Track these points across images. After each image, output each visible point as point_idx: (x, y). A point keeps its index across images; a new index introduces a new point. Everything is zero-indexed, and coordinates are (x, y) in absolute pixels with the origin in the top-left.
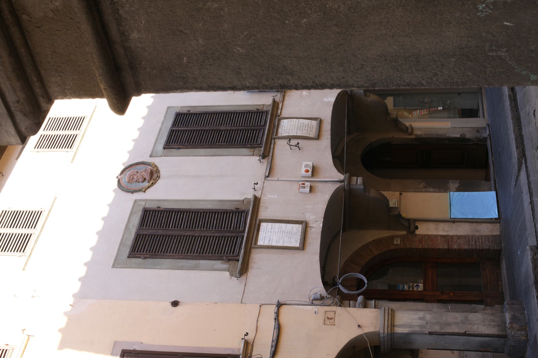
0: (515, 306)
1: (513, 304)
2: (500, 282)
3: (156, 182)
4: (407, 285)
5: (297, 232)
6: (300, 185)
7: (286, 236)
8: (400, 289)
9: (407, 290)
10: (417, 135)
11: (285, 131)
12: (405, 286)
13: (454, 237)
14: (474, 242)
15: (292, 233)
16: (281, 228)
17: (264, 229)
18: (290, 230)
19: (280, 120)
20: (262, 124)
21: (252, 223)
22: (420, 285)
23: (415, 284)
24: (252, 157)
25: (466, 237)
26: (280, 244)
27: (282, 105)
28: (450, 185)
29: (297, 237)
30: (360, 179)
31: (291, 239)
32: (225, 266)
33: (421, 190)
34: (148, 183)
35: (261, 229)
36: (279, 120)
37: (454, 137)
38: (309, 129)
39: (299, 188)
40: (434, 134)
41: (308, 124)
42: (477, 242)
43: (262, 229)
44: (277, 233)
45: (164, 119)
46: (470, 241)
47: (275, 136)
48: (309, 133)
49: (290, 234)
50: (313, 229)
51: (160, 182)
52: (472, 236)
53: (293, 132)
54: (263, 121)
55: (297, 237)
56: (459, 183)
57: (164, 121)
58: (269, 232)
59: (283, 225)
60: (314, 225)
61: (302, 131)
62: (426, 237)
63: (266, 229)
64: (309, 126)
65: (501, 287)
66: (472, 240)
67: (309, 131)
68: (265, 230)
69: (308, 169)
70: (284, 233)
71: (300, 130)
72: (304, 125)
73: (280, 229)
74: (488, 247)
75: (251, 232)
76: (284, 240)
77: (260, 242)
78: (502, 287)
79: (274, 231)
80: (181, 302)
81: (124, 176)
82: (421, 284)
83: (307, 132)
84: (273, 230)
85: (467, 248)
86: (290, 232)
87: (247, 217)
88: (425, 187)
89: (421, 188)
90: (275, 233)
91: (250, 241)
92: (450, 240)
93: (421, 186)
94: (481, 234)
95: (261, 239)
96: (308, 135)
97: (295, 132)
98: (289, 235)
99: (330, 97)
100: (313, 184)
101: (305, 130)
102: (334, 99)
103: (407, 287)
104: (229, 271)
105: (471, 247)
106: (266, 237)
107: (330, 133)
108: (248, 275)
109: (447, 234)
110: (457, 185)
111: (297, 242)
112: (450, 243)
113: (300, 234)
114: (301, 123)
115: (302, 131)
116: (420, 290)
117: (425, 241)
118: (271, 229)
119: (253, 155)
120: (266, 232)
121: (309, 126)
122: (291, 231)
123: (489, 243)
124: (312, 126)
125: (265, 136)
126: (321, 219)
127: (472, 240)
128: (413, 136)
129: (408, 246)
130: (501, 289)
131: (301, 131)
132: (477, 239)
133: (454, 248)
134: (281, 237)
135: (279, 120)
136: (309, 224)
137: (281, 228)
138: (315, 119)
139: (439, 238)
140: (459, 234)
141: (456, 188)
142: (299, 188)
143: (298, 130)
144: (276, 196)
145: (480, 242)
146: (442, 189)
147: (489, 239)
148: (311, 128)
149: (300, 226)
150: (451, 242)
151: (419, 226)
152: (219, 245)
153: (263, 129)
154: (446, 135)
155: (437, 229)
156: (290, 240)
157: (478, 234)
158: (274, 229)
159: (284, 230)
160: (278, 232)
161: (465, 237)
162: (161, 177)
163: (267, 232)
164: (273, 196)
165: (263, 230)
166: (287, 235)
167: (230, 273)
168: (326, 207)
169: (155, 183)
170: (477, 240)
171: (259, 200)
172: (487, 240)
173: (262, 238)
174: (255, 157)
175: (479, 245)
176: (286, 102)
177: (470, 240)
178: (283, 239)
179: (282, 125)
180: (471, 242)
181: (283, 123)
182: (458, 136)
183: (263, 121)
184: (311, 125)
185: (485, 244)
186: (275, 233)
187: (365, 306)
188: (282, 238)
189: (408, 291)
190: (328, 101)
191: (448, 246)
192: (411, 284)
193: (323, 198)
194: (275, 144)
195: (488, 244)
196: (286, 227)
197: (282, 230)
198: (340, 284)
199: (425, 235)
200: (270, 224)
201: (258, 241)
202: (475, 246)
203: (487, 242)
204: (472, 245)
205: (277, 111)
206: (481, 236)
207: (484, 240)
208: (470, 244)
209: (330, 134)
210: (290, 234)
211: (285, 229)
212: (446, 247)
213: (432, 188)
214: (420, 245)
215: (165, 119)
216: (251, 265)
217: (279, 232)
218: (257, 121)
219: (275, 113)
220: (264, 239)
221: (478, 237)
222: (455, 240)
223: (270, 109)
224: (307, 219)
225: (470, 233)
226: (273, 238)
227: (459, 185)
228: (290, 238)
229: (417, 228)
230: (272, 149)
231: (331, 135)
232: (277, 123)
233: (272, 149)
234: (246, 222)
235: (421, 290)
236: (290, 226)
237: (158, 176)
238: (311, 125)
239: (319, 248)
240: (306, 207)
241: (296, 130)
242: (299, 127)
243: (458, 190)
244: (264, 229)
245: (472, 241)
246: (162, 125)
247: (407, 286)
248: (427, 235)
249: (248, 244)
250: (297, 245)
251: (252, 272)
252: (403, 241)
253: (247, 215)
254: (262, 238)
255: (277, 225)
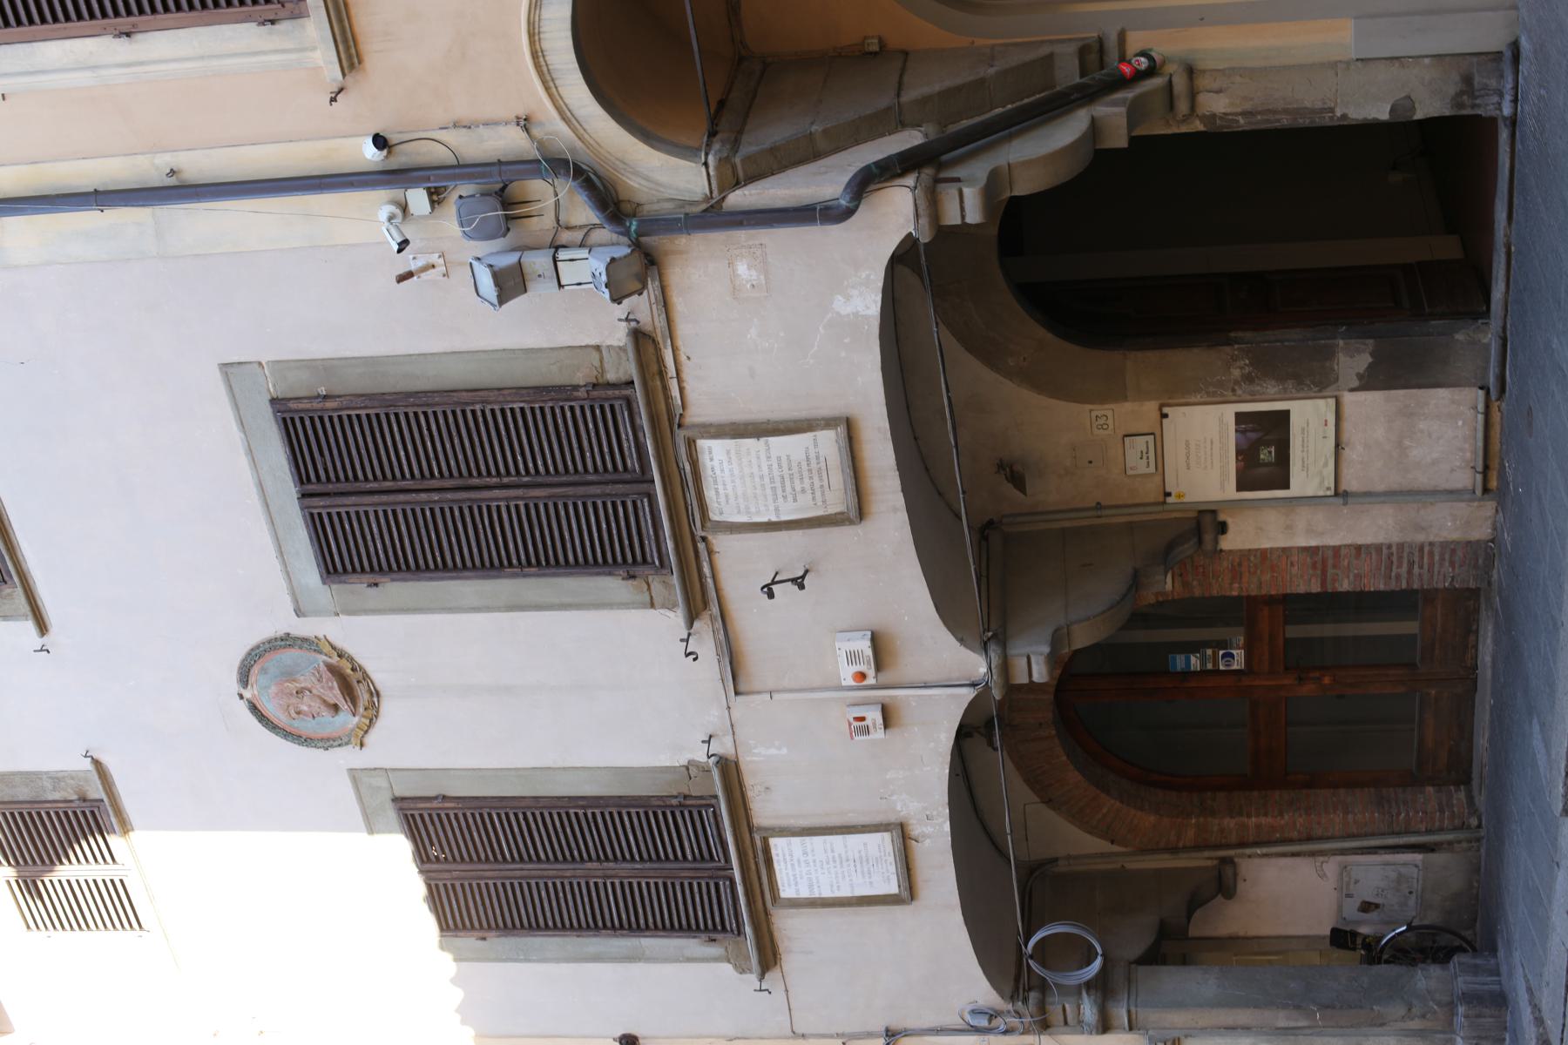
0: (1483, 1020)
1: (1478, 1016)
2: (1472, 638)
3: (378, 712)
4: (1198, 655)
5: (883, 854)
6: (850, 725)
7: (853, 869)
8: (1179, 669)
9: (1199, 669)
10: (1214, 116)
11: (732, 500)
12: (1193, 659)
13: (1343, 552)
14: (1405, 565)
15: (867, 860)
16: (833, 851)
17: (784, 855)
18: (860, 852)
19: (694, 441)
20: (633, 462)
21: (743, 842)
22: (1234, 652)
23: (1221, 652)
24: (652, 611)
25: (1381, 549)
26: (845, 892)
27: (675, 350)
28: (1338, 364)
29: (888, 871)
30: (1038, 664)
31: (870, 877)
32: (714, 950)
33: (1234, 390)
34: (354, 715)
35: (775, 858)
36: (690, 446)
37: (1365, 119)
38: (817, 484)
39: (851, 734)
40: (1286, 111)
41: (808, 459)
42: (1416, 566)
43: (777, 855)
44: (825, 866)
45: (243, 436)
46: (1392, 562)
47: (703, 526)
48: (824, 502)
49: (865, 864)
50: (928, 842)
51: (387, 707)
52: (1401, 546)
53: (762, 508)
54: (630, 448)
55: (888, 871)
56: (1372, 354)
57: (249, 445)
58: (803, 864)
59: (837, 840)
60: (924, 829)
61: (795, 500)
62: (1252, 558)
63: (791, 855)
64: (814, 465)
65: (1473, 651)
66: (1400, 558)
67: (818, 494)
68: (788, 858)
69: (862, 668)
70: (845, 864)
71: (785, 497)
72: (795, 469)
73: (830, 855)
74: (1447, 584)
75: (749, 869)
76: (851, 880)
77: (786, 892)
78: (1477, 650)
79: (814, 861)
80: (644, 1038)
81: (259, 692)
82: (1239, 651)
83: (814, 499)
84: (810, 858)
85: (1382, 587)
86: (861, 857)
87: (721, 826)
88: (1249, 379)
89: (1236, 382)
90: (818, 864)
91: (758, 892)
92: (1330, 562)
93: (1236, 373)
94: (1432, 538)
95: (786, 882)
96: (820, 512)
97: (772, 508)
98: (862, 866)
99: (855, 292)
100: (886, 701)
101: (803, 491)
102: (875, 302)
103: (1198, 662)
104: (729, 961)
105: (1393, 586)
106: (798, 879)
107: (897, 482)
108: (784, 969)
109: (1321, 544)
110: (1363, 361)
111: (889, 882)
112: (1330, 571)
113: (891, 859)
114: (779, 459)
115: (795, 500)
116: (1235, 667)
117: (1252, 570)
118: (805, 853)
119: (652, 605)
120: (793, 865)
121: (814, 465)
122: (863, 854)
123: (1454, 569)
124: (823, 465)
125: (670, 545)
126: (940, 809)
127: (1400, 558)
128: (1198, 126)
129: (1197, 592)
130: (1472, 659)
131: (790, 498)
132: (1417, 554)
133: (1340, 589)
134: (840, 875)
135: (691, 443)
136: (910, 828)
137: (833, 851)
138: (829, 423)
139: (1295, 559)
140: (1360, 541)
141: (1360, 376)
142: (851, 734)
143: (781, 500)
144: (784, 751)
145: (1426, 566)
146: (1308, 382)
147: (1453, 551)
148: (824, 474)
149: (887, 836)
150: (1335, 566)
151: (1229, 521)
152: (673, 904)
153: (645, 500)
154: (1332, 110)
155: (1289, 527)
156: (868, 880)
157: (1421, 538)
158: (814, 855)
159: (844, 856)
160: (828, 863)
161: (1378, 548)
162: (382, 693)
163: (796, 864)
164: (773, 751)
165: (781, 858)
166: (855, 866)
167: (735, 967)
168: (947, 771)
169: (376, 717)
170: (1416, 559)
171: (733, 764)
172: (1447, 556)
173: (789, 880)
174: (662, 611)
175: (1420, 575)
176: (683, 329)
177: (1395, 559)
178: (847, 879)
179: (709, 472)
180: (1394, 567)
181: (711, 460)
182: (1383, 115)
183: (630, 448)
184: (818, 458)
185: (1439, 572)
186: (818, 864)
187: (1105, 1026)
188: (844, 877)
189: (1204, 673)
190: (856, 314)
191: (1324, 583)
192: (1209, 652)
193: (932, 745)
194: (710, 552)
195: (1450, 570)
196: (846, 847)
197: (836, 855)
198: (1031, 957)
199: (1250, 550)
200: (796, 841)
201: (778, 890)
202: (1408, 583)
203: (1447, 564)
204: (1398, 577)
205: (665, 388)
206: (1431, 544)
207: (1437, 558)
208: (1393, 574)
209: (900, 488)
210: (865, 864)
211: (846, 852)
212: (1315, 588)
213: (1273, 382)
214: (1236, 585)
215: (245, 433)
216: (783, 945)
217: (831, 863)
218: (606, 449)
219: (663, 406)
220: (792, 882)
221: (1421, 548)
222: (1346, 563)
223: (630, 369)
224: (900, 812)
225: (1396, 538)
226: (817, 878)
227: (1370, 360)
228: (867, 876)
229: (1223, 528)
230: (710, 581)
231: (903, 491)
232: (688, 468)
233: (710, 581)
234: (724, 837)
235: (1239, 668)
236: (855, 840)
237: (371, 694)
238: (818, 458)
239: (957, 892)
240: (888, 777)
241: (770, 499)
242: (778, 485)
243: (1368, 382)
244: (784, 855)
245: (1400, 566)
246: (257, 471)
247: (1196, 657)
248: (1256, 550)
249: (754, 902)
250: (892, 888)
251: (792, 960)
252: (1181, 575)
253: (719, 819)
254: (789, 880)
255: (818, 840)
